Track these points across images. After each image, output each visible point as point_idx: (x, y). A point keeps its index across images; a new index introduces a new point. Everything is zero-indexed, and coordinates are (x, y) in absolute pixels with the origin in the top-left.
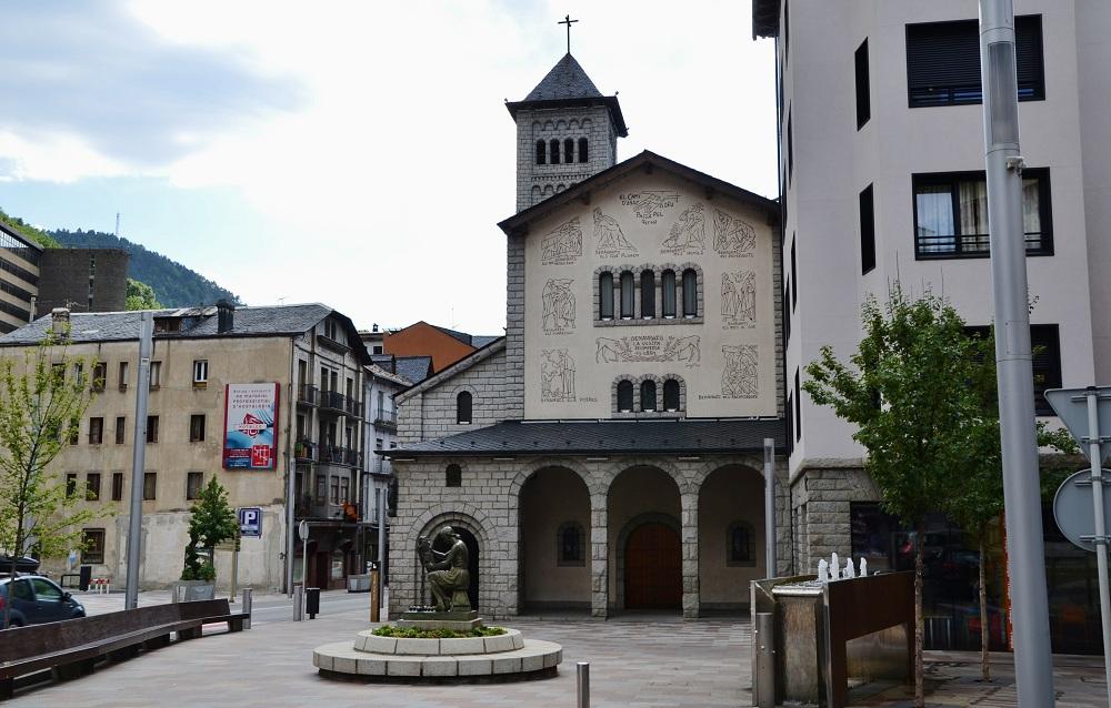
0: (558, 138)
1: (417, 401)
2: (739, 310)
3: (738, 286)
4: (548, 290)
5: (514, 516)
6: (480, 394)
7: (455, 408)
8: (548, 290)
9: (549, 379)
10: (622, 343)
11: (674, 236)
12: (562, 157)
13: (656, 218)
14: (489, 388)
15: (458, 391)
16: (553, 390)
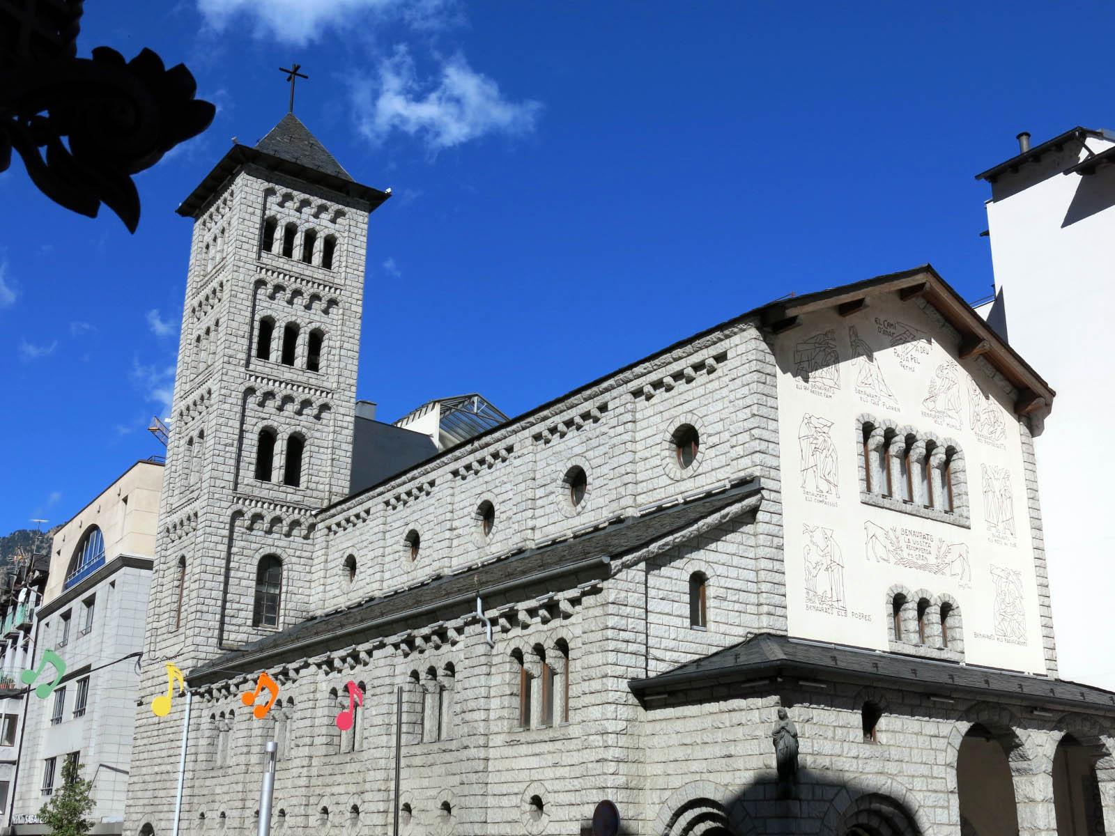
0: (298, 222)
1: (637, 573)
2: (1000, 521)
3: (997, 485)
4: (805, 431)
5: (955, 801)
6: (723, 582)
7: (687, 598)
8: (805, 431)
9: (814, 572)
10: (891, 533)
11: (932, 397)
12: (298, 252)
13: (911, 364)
14: (733, 573)
15: (692, 568)
16: (820, 593)
